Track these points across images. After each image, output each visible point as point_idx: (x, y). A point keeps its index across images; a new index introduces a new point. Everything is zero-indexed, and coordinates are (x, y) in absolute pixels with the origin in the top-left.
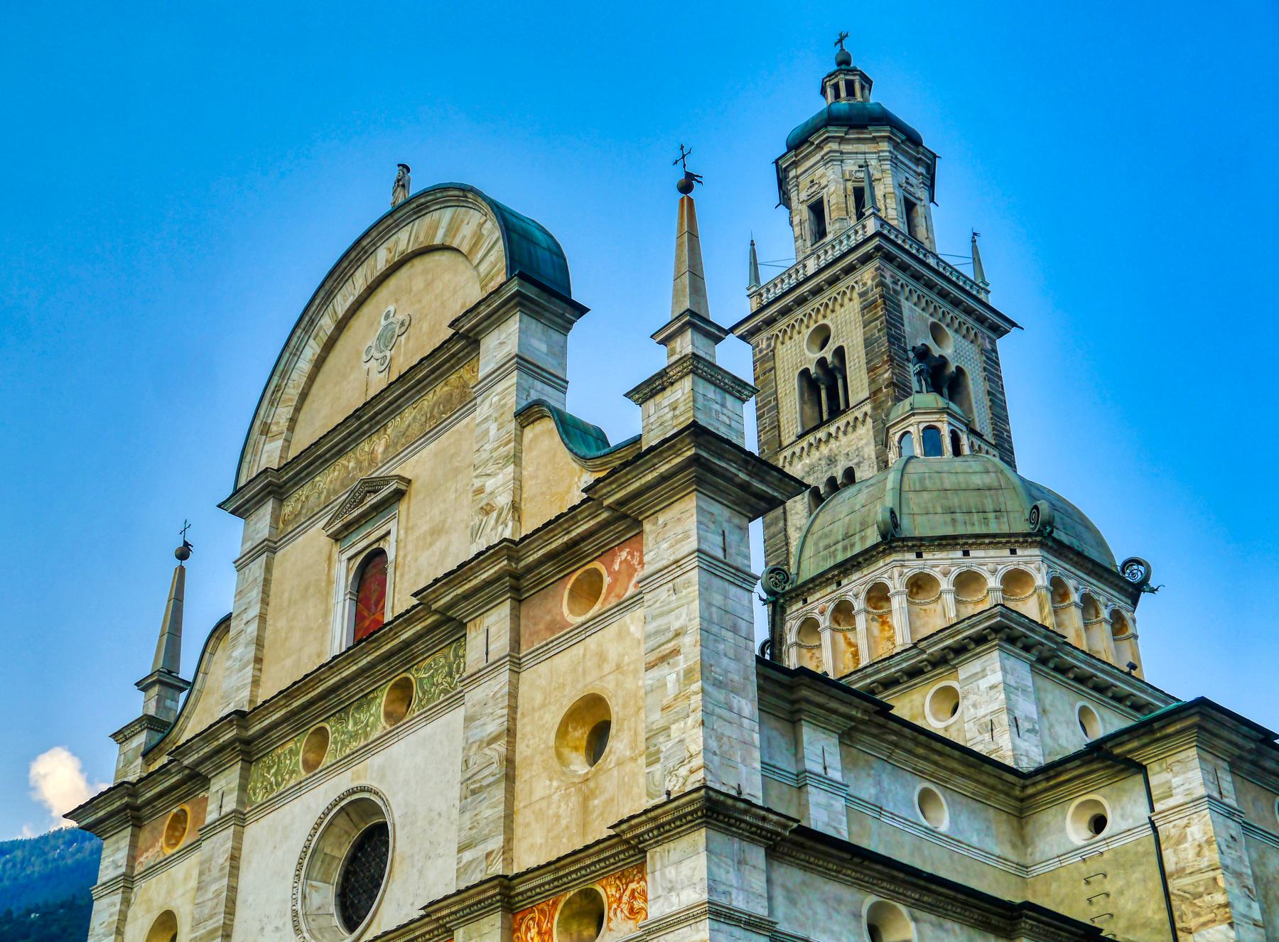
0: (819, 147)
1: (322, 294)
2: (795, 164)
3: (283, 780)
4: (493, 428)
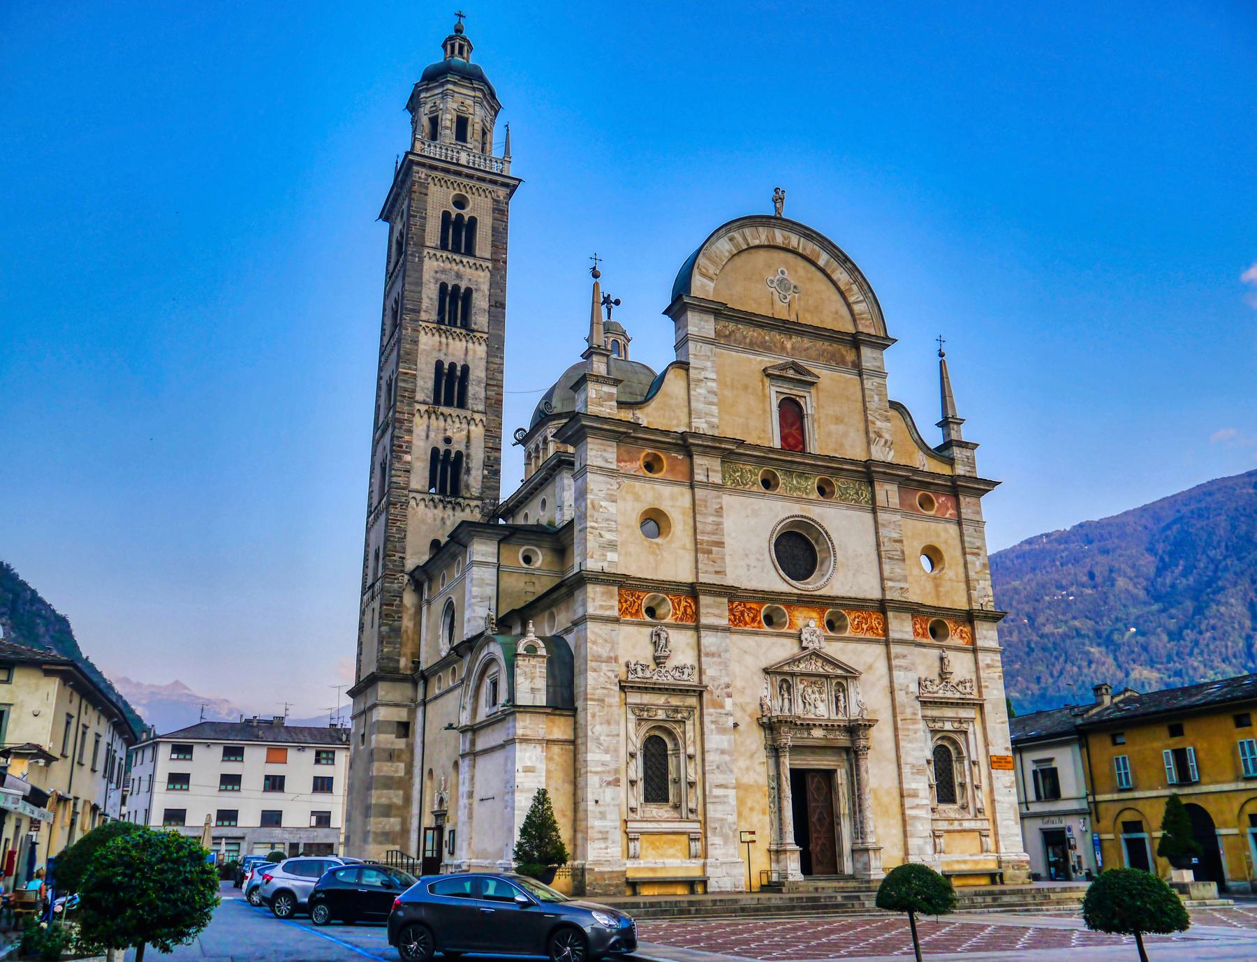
0: (474, 89)
1: (741, 222)
2: (455, 83)
3: (747, 484)
4: (876, 398)
